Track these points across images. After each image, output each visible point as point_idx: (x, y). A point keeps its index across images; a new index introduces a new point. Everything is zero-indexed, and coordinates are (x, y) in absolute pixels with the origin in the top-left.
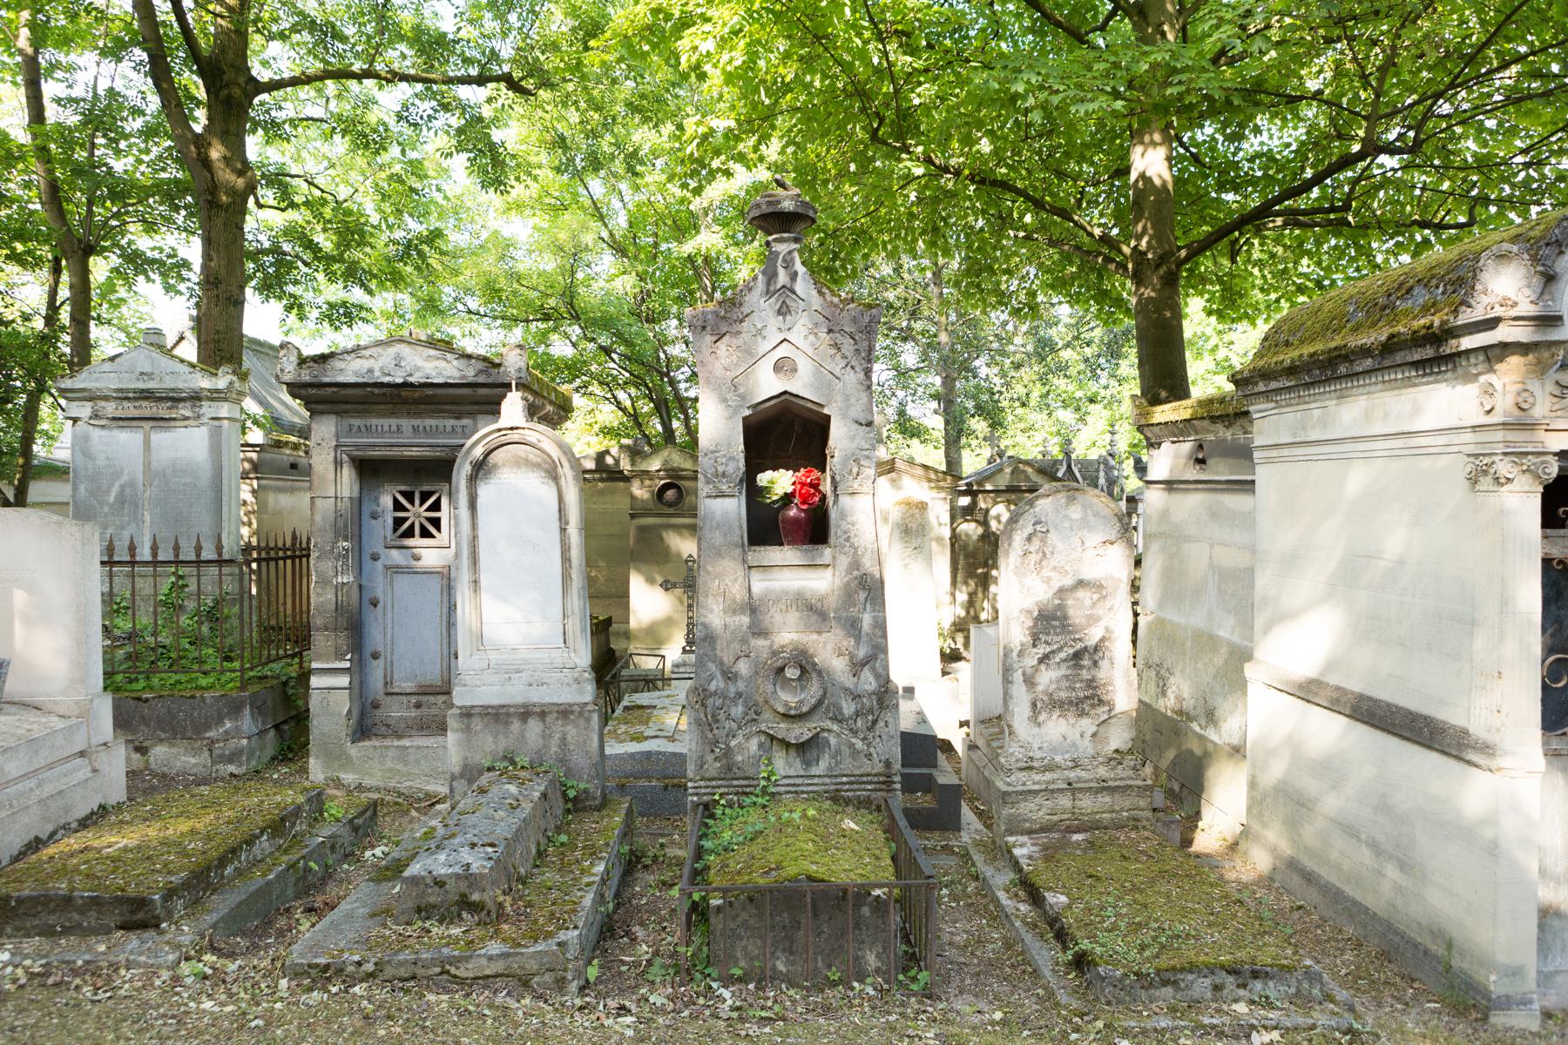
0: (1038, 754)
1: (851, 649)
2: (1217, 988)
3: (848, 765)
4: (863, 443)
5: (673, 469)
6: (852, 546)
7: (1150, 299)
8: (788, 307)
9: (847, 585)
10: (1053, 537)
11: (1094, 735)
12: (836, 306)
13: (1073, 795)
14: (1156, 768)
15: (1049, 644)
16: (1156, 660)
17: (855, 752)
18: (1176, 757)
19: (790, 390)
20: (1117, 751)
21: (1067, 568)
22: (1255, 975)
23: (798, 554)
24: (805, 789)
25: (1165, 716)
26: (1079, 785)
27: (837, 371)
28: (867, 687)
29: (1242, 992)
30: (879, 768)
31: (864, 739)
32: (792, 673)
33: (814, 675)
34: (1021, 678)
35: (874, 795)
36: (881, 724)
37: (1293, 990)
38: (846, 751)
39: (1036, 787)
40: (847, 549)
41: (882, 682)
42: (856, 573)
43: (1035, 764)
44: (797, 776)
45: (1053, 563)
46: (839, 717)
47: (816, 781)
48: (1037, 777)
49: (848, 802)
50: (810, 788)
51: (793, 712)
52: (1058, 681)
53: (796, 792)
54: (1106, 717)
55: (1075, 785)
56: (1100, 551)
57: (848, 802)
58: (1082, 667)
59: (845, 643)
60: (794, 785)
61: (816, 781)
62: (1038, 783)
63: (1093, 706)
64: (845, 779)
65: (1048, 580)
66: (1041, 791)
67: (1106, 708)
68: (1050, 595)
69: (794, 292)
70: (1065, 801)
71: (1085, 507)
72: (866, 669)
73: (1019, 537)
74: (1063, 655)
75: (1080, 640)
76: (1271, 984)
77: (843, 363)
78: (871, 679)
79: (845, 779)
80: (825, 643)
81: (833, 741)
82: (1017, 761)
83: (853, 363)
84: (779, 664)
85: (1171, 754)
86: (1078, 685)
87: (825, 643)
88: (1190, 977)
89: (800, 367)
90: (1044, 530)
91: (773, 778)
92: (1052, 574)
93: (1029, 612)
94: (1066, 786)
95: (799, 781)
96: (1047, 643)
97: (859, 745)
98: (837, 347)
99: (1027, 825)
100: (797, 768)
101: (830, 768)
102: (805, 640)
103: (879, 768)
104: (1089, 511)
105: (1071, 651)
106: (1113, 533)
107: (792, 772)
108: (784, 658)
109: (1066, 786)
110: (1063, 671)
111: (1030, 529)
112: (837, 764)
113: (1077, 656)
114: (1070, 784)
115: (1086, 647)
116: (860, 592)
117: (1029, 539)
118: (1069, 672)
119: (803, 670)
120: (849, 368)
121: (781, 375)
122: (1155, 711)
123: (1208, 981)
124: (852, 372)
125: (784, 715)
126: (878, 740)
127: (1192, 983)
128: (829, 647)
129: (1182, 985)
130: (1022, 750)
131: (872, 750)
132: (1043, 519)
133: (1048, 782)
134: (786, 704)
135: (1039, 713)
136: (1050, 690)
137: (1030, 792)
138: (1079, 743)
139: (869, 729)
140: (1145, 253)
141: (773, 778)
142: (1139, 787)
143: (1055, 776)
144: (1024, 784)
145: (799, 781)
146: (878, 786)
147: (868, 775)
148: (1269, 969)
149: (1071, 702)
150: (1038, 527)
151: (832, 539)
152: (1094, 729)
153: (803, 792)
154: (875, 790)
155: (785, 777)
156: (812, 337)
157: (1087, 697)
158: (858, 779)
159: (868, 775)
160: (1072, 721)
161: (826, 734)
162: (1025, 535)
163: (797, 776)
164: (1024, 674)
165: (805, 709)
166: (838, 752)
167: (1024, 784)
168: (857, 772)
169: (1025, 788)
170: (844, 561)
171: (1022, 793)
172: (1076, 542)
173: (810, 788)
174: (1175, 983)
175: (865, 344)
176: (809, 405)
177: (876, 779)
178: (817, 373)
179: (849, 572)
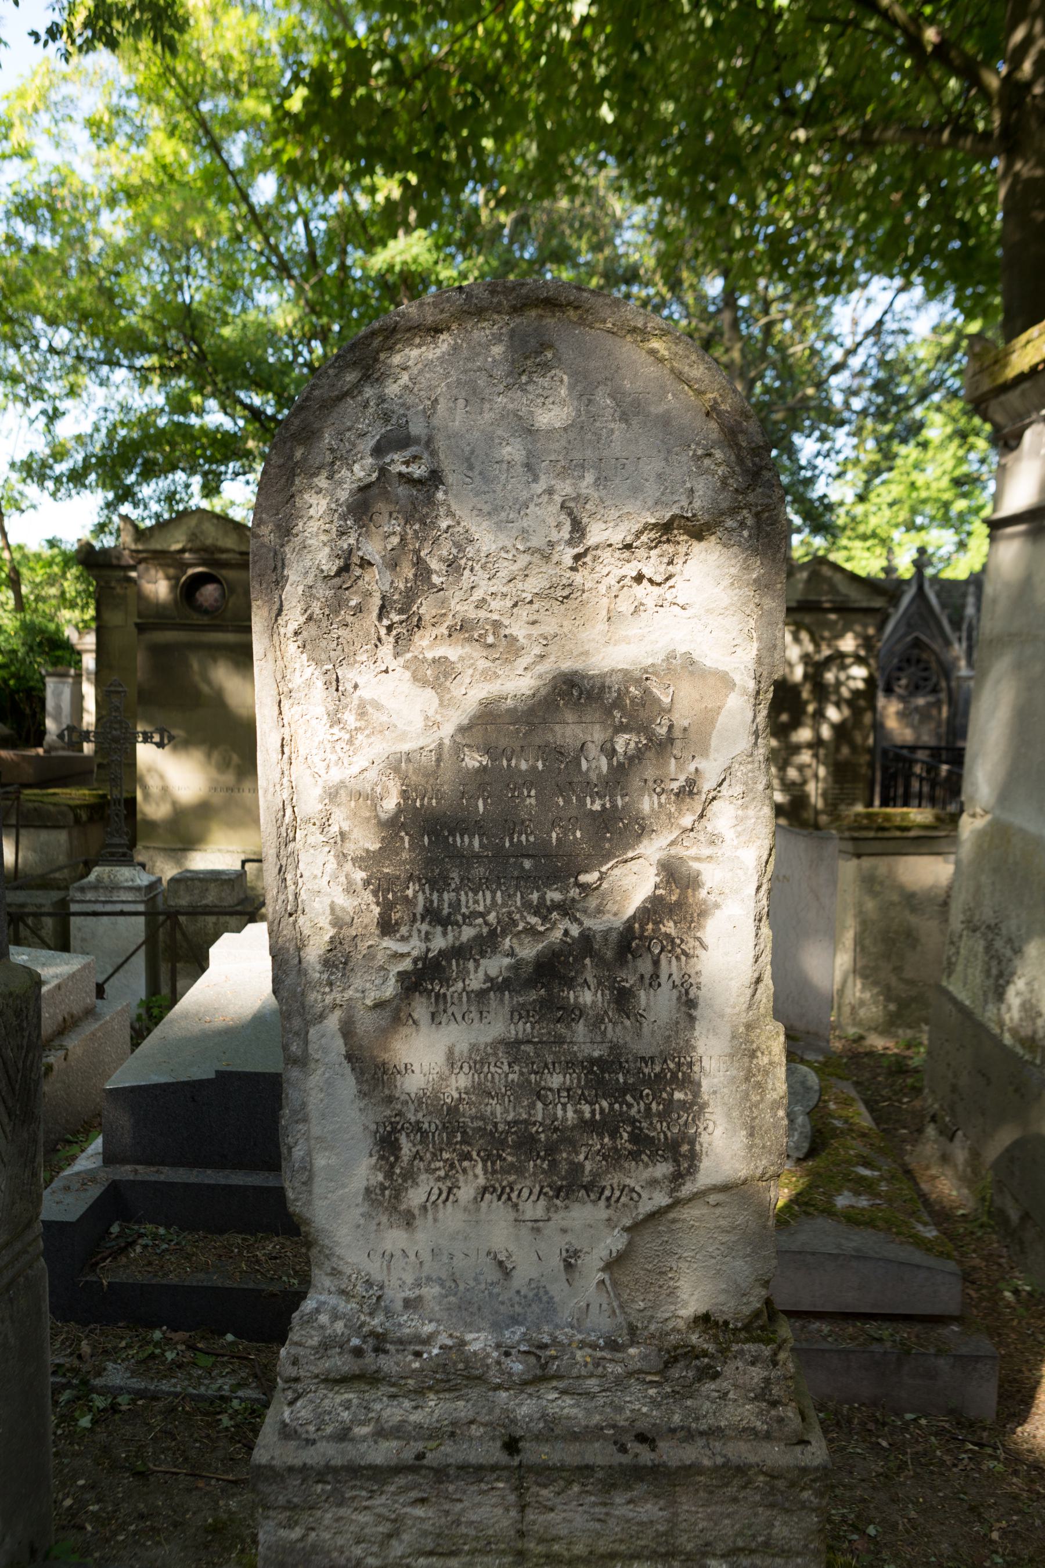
0: (410, 1324)
5: (205, 549)
7: (1032, 182)
11: (615, 1264)
13: (519, 1489)
14: (975, 1155)
16: (987, 914)
18: (1017, 1144)
20: (704, 1320)
21: (518, 629)
25: (997, 1041)
34: (339, 1045)
39: (382, 1453)
43: (388, 1364)
48: (394, 1413)
52: (478, 1060)
54: (661, 1199)
56: (652, 566)
58: (572, 1013)
62: (397, 1432)
63: (614, 1158)
66: (398, 1470)
67: (662, 1169)
74: (495, 965)
85: (1005, 1137)
86: (555, 1081)
90: (418, 471)
92: (452, 652)
93: (373, 800)
94: (493, 1453)
96: (433, 916)
105: (528, 951)
111: (362, 470)
114: (512, 1446)
118: (522, 1029)
122: (980, 1028)
130: (345, 1307)
132: (417, 428)
133: (434, 1434)
135: (410, 1175)
137: (356, 1471)
138: (558, 1289)
140: (1028, 85)
142: (773, 1475)
143: (462, 1409)
144: (343, 1435)
149: (527, 1143)
152: (615, 1242)
157: (588, 1126)
160: (533, 1209)
164: (347, 1030)
171: (325, 1473)
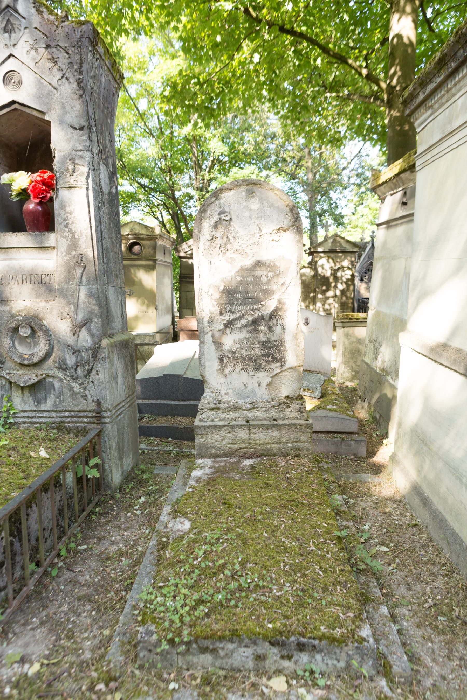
0: (225, 398)
1: (71, 314)
2: (259, 658)
3: (69, 404)
4: (77, 145)
5: (135, 234)
6: (70, 231)
7: (396, 117)
8: (12, 25)
9: (67, 263)
10: (235, 225)
11: (269, 384)
12: (52, 23)
13: (249, 430)
14: (369, 403)
15: (233, 313)
16: (374, 337)
17: (74, 394)
18: (379, 398)
19: (16, 100)
20: (287, 397)
21: (248, 251)
22: (301, 647)
23: (30, 238)
24: (37, 420)
25: (376, 372)
26: (254, 423)
27: (55, 83)
28: (85, 344)
29: (286, 663)
30: (92, 406)
31: (80, 385)
32: (24, 332)
33: (40, 334)
34: (211, 339)
35: (89, 427)
36: (94, 372)
37: (342, 664)
38: (67, 393)
39: (221, 423)
40: (66, 234)
41: (96, 340)
42: (74, 253)
43: (222, 406)
44: (31, 411)
45: (236, 246)
46: (64, 367)
47: (45, 414)
48: (223, 416)
49: (69, 431)
50: (41, 420)
51: (26, 362)
52: (240, 342)
53: (31, 423)
54: (278, 371)
55: (251, 423)
56: (276, 237)
57: (69, 431)
58: (259, 332)
59: (67, 309)
60: (28, 417)
61: (45, 414)
62: (223, 420)
63: (268, 362)
64: (67, 414)
65: (232, 260)
66: (224, 426)
67: (279, 364)
68: (233, 273)
69: (16, 11)
70: (243, 434)
71: (262, 200)
72: (84, 329)
73: (207, 225)
74: (244, 322)
75: (258, 310)
76: (318, 657)
77: (59, 75)
78: (88, 338)
79: (67, 414)
80: (52, 309)
81: (57, 385)
82: (208, 403)
83: (67, 75)
84: (14, 325)
85: (376, 396)
86: (256, 346)
87: (52, 309)
88: (230, 646)
89: (24, 80)
90: (227, 218)
91: (12, 412)
92: (235, 256)
93: (218, 287)
94: (244, 423)
95: (33, 414)
96: (231, 311)
97: (77, 388)
98: (54, 60)
99: (214, 451)
100: (30, 405)
101: (55, 405)
102: (36, 307)
103: (92, 406)
104: (265, 203)
105: (250, 318)
106: (286, 221)
107: (27, 408)
108: (18, 320)
109: (244, 423)
110: (244, 334)
111: (216, 218)
112: (61, 402)
113: (255, 322)
114: (248, 421)
115: (262, 316)
116: (77, 269)
117: (216, 226)
118: (249, 335)
119: (33, 332)
120: (64, 80)
121: (10, 87)
122: (371, 368)
123: (249, 652)
124: (67, 83)
125: (20, 364)
126: (91, 384)
127: (232, 652)
128: (55, 312)
129: (222, 653)
130: (212, 395)
131: (87, 392)
132: (227, 210)
133: (231, 420)
134: (21, 356)
135: (226, 366)
136: (234, 349)
137: (216, 426)
138: (257, 390)
139: (85, 377)
140: (395, 87)
141: (12, 412)
142: (301, 426)
143: (237, 415)
144: (212, 421)
145: (33, 414)
146: (92, 420)
147: (85, 411)
148: (317, 642)
149: (250, 359)
150: (223, 217)
151: (57, 226)
152: (269, 380)
153: (37, 423)
154: (90, 423)
155: (22, 411)
156: (33, 52)
157: (263, 355)
158: (77, 414)
159: (85, 411)
160: (252, 373)
161: (51, 380)
162: (212, 223)
163: (31, 411)
164: (213, 336)
165: (35, 360)
166: (61, 393)
167: (212, 421)
168: (76, 409)
169: (212, 424)
170: (64, 244)
171: (209, 427)
172: (254, 229)
173: (41, 420)
174: (214, 651)
175: (77, 57)
176: (35, 113)
177: (90, 414)
178: (39, 84)
179: (68, 252)
